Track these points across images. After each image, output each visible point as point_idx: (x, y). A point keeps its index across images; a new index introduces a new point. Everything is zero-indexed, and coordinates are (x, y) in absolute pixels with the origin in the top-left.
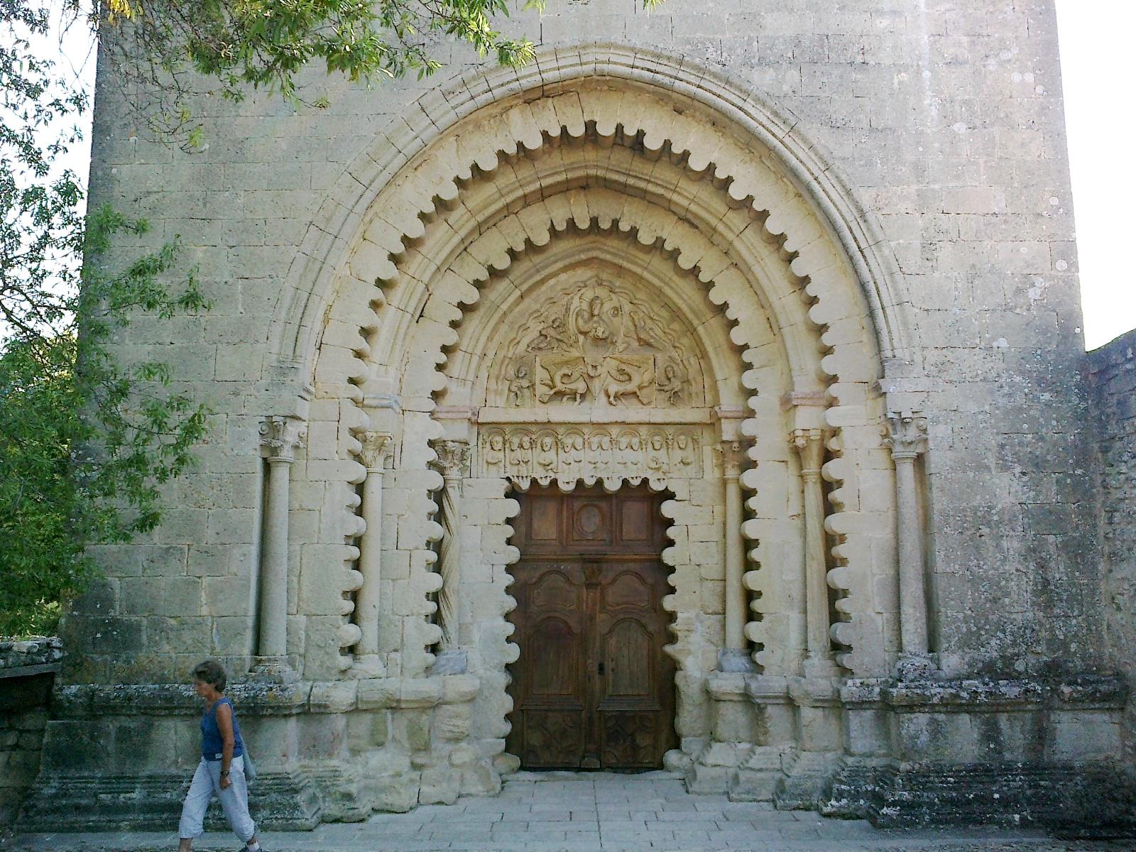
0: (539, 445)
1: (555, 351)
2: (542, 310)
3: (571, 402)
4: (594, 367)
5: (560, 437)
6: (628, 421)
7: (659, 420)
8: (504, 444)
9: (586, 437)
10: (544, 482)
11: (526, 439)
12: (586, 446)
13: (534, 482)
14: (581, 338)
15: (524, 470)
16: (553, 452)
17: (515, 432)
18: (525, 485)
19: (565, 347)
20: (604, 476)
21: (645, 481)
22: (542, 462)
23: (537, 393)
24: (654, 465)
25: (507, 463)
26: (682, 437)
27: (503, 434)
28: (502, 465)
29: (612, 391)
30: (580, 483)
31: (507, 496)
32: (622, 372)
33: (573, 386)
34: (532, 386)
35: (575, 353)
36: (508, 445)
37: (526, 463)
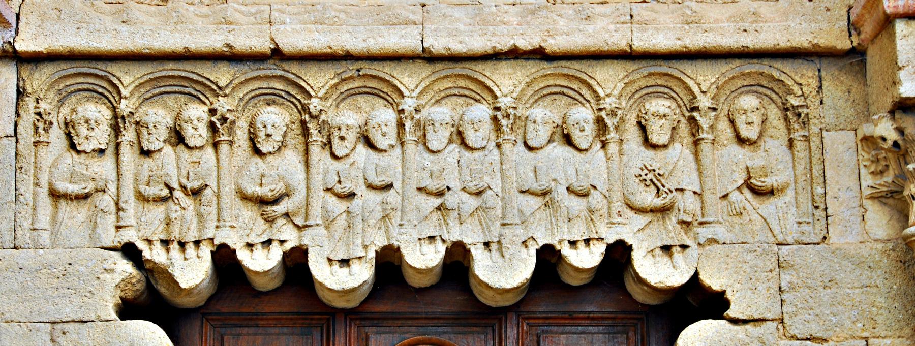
0: (241, 135)
5: (315, 104)
6: (554, 44)
7: (663, 41)
9: (408, 104)
10: (261, 262)
11: (196, 112)
13: (224, 258)
17: (155, 90)
18: (192, 272)
20: (471, 237)
21: (619, 254)
22: (252, 189)
24: (648, 198)
25: (128, 193)
26: (749, 101)
27: (109, 94)
28: (106, 201)
31: (128, 309)
36: (128, 135)
37: (196, 193)
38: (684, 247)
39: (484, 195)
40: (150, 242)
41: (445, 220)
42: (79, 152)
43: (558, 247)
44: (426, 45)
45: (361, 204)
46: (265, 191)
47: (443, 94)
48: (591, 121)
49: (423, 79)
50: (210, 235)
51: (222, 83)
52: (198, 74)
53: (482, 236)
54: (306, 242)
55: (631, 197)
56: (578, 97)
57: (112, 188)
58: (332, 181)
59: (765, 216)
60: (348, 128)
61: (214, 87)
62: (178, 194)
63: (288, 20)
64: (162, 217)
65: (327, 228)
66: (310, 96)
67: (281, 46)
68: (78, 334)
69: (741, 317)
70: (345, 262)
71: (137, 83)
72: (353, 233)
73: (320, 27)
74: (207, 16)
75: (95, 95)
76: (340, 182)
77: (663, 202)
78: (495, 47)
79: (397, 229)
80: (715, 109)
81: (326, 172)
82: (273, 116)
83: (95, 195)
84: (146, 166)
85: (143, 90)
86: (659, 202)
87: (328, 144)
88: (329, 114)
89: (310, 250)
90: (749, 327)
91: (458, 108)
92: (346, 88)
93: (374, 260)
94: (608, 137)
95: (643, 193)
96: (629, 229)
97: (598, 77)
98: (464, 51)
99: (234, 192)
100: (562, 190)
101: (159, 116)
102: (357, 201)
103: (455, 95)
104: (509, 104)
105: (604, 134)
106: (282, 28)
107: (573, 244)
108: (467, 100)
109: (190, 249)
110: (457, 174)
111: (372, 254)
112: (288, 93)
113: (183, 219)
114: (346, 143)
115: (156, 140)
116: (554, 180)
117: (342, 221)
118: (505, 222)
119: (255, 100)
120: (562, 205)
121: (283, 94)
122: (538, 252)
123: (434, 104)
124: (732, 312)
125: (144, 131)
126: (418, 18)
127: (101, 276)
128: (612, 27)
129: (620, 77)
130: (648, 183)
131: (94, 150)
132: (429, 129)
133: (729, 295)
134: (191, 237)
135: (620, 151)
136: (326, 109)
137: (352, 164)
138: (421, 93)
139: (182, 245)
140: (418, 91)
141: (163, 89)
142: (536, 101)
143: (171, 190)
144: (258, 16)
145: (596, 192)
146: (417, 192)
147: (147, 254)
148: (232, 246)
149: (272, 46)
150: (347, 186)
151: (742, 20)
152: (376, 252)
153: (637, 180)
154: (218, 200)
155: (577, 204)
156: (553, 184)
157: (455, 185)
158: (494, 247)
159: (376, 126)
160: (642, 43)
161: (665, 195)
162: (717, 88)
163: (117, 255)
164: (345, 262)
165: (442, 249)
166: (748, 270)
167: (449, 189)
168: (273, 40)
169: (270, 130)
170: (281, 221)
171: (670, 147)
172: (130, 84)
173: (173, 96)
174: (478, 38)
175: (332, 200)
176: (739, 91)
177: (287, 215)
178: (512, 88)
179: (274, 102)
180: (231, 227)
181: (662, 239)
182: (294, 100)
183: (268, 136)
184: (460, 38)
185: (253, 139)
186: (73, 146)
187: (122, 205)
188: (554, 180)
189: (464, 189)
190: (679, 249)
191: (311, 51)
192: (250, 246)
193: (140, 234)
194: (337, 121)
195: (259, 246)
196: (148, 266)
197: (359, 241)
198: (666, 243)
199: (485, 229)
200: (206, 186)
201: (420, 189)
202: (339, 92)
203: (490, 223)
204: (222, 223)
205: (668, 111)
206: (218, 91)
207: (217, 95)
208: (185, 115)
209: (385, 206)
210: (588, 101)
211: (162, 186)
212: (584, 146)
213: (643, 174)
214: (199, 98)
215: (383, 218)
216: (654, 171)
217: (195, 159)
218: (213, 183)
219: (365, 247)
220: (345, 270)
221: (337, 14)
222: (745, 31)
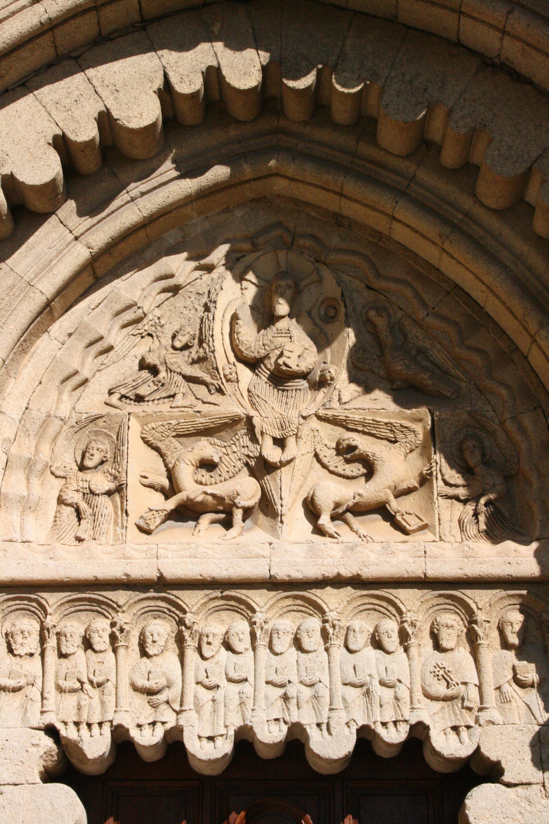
0: (134, 641)
1: (179, 401)
2: (147, 306)
3: (219, 529)
4: (280, 443)
5: (189, 618)
8: (43, 640)
10: (147, 738)
11: (101, 626)
12: (262, 642)
14: (245, 374)
15: (93, 705)
16: (171, 658)
18: (96, 746)
19: (201, 390)
20: (306, 718)
22: (141, 682)
23: (131, 507)
24: (440, 689)
29: (326, 504)
30: (244, 741)
31: (49, 776)
32: (346, 452)
33: (221, 489)
34: (119, 490)
35: (230, 406)
36: (52, 642)
37: (99, 685)
38: (468, 727)
39: (316, 687)
40: (65, 723)
41: (287, 706)
42: (15, 655)
43: (373, 727)
44: (272, 573)
45: (223, 694)
46: (151, 684)
47: (285, 610)
48: (397, 631)
49: (270, 598)
50: (110, 718)
51: (120, 603)
52: (103, 597)
53: (315, 718)
54: (181, 722)
55: (428, 689)
56: (386, 612)
57: (39, 682)
58: (202, 677)
59: (528, 703)
60: (214, 635)
61: (115, 606)
62: (87, 686)
63: (170, 555)
64: (75, 704)
65: (198, 712)
66: (185, 612)
67: (165, 574)
68: (12, 794)
69: (513, 781)
70: (211, 739)
71: (59, 603)
72: (217, 716)
73: (193, 560)
74: (110, 553)
75: (28, 612)
76: (207, 677)
77: (452, 692)
78: (324, 575)
79: (250, 712)
80: (488, 622)
81: (197, 669)
82: (158, 627)
83: (26, 688)
84: (64, 665)
85: (63, 608)
86: (449, 692)
87: (199, 649)
88: (201, 626)
89: (185, 729)
90: (519, 789)
91: (296, 620)
92: (212, 605)
93: (233, 737)
94: (409, 642)
95: (437, 685)
96: (428, 713)
97: (401, 597)
98: (301, 577)
99: (128, 685)
100: (376, 682)
101: (75, 627)
102: (221, 691)
103: (294, 611)
104: (335, 618)
105: (406, 641)
106: (165, 561)
107: (384, 724)
108: (303, 614)
109: (96, 729)
110: (296, 670)
111: (232, 733)
112: (169, 610)
113: (90, 705)
114: (212, 647)
115: (73, 645)
116: (369, 675)
117: (209, 707)
118: (332, 707)
119: (145, 615)
120: (375, 694)
121: (166, 610)
122: (358, 731)
123: (278, 617)
124: (506, 778)
125: (63, 638)
126: (267, 553)
127: (29, 749)
128: (410, 560)
129: (418, 597)
130: (440, 677)
131: (26, 654)
132: (275, 636)
133: (504, 765)
134: (95, 719)
135: (419, 653)
136: (197, 621)
137: (216, 663)
138: (269, 609)
139: (89, 725)
140: (266, 607)
141: (78, 608)
142: (355, 615)
143: (82, 683)
144: (148, 553)
145: (401, 684)
146: (265, 685)
147: (63, 732)
148: (126, 726)
149: (158, 575)
150: (213, 680)
151: (507, 555)
152: (235, 731)
153: (432, 675)
154: (116, 691)
155: (387, 694)
156: (368, 678)
157: (295, 679)
158: (324, 727)
159: (235, 634)
160: (433, 572)
161: (453, 687)
162: (490, 606)
163: (42, 733)
164: (211, 739)
165: (285, 728)
166: (517, 745)
167: (290, 682)
168: (159, 570)
169: (156, 638)
170: (164, 707)
171: (456, 650)
172: (54, 604)
173: (85, 613)
174: (311, 568)
175: (201, 690)
176: (506, 608)
177: (168, 702)
178: (337, 605)
179: (159, 617)
180: (126, 711)
181: (451, 721)
182: (174, 615)
183: (154, 642)
184: (298, 568)
185: (142, 645)
186: (11, 651)
187: (45, 695)
188: (369, 675)
189: (301, 682)
190: (465, 729)
191: (186, 578)
192: (139, 726)
193: (59, 717)
194: (206, 631)
195: (147, 726)
196: (63, 742)
197: (222, 723)
198: (454, 724)
199: (317, 711)
200: (108, 680)
201: (267, 683)
202: (207, 609)
203: (321, 708)
204: (119, 709)
205: (454, 623)
206: (118, 609)
207: (117, 612)
208: (94, 626)
209: (241, 695)
210: (394, 615)
211: (75, 681)
212: (391, 649)
213: (436, 670)
214: (104, 615)
215: (240, 704)
216: (444, 668)
217: (100, 660)
218: (113, 679)
219: (226, 727)
220: (211, 744)
221: (206, 551)
222: (509, 563)
